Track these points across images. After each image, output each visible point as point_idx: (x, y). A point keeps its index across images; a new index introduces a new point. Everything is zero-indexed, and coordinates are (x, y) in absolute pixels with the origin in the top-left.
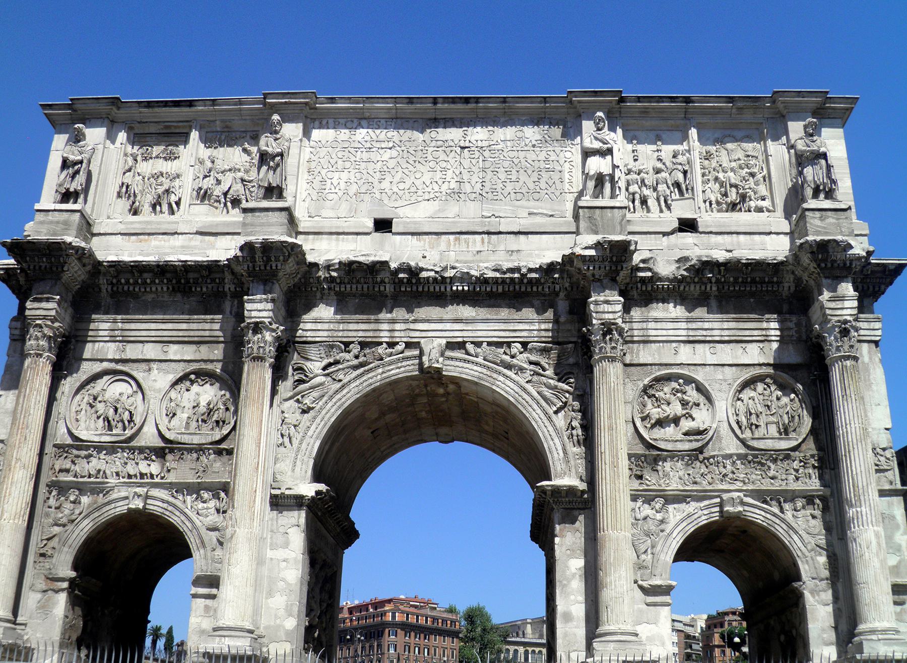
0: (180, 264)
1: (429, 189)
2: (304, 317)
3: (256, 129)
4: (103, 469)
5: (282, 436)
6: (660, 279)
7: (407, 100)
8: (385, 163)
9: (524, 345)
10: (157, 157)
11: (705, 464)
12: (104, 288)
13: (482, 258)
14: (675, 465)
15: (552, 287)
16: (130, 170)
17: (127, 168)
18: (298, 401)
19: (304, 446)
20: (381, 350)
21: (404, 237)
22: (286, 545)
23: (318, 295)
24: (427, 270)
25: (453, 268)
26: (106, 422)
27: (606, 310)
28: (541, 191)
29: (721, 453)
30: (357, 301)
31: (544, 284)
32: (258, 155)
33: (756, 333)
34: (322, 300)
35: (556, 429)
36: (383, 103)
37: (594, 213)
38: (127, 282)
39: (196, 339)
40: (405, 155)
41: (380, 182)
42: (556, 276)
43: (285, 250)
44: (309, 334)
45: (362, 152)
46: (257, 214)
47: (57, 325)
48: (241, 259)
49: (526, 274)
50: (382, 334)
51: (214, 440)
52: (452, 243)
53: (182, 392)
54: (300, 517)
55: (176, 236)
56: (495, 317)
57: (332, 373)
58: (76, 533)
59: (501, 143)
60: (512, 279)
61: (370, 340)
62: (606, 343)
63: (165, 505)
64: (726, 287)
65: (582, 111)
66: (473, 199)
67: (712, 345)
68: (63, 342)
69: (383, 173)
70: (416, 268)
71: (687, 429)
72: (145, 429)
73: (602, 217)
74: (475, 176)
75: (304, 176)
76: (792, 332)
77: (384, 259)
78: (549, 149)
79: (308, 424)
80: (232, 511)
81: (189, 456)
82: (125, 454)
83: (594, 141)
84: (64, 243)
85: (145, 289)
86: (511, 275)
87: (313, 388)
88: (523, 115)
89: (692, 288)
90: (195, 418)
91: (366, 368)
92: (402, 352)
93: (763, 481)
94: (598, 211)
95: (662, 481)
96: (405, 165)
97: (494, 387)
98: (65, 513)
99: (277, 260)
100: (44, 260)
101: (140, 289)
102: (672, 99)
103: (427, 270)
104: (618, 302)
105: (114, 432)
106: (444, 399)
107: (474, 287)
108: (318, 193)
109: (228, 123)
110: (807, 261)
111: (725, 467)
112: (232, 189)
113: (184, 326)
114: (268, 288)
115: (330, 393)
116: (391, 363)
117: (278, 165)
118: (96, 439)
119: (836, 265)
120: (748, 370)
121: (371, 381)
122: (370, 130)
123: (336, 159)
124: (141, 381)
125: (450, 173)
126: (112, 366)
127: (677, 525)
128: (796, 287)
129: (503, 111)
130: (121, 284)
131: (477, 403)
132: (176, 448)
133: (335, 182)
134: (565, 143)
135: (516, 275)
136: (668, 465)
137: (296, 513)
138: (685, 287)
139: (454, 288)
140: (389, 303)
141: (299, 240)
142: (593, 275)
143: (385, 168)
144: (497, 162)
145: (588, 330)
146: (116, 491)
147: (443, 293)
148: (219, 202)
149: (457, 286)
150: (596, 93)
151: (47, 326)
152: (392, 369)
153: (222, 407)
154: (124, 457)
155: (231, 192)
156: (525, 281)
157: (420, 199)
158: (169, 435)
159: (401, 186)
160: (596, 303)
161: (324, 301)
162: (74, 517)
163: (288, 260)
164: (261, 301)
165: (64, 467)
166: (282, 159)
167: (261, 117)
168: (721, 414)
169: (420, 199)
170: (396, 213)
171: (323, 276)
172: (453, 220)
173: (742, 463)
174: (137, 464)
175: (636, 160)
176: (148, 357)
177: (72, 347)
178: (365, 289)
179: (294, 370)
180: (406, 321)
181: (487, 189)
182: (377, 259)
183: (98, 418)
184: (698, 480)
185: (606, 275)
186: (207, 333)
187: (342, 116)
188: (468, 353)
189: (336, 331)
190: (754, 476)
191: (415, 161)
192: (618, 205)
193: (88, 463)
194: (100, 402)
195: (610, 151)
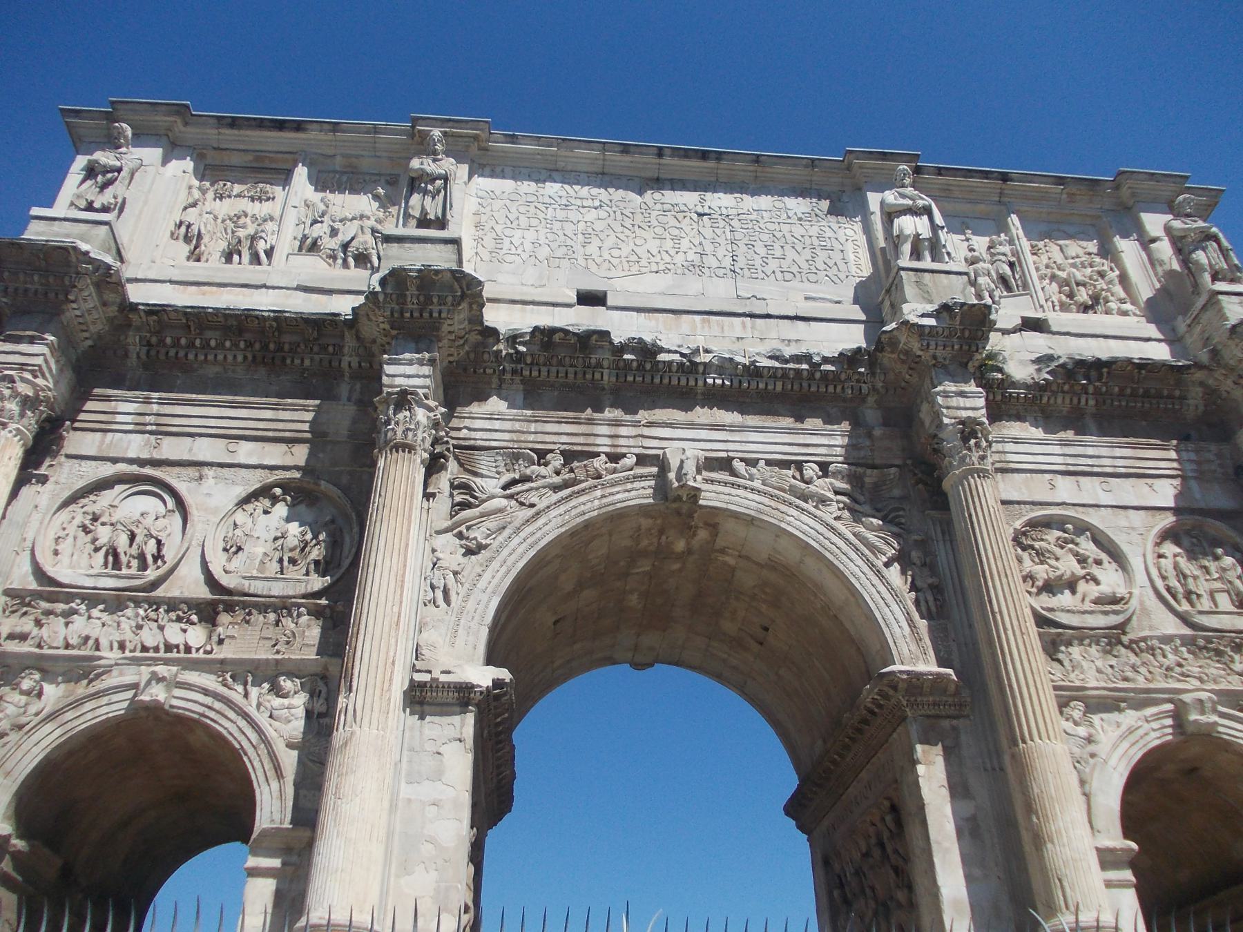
0: (272, 314)
1: (658, 259)
4: (94, 635)
5: (433, 587)
6: (1014, 384)
7: (621, 148)
8: (589, 224)
10: (238, 196)
11: (1133, 651)
14: (1086, 651)
16: (194, 205)
17: (191, 200)
18: (460, 536)
19: (471, 605)
20: (599, 463)
22: (437, 775)
24: (669, 352)
25: (707, 351)
26: (111, 559)
29: (1157, 633)
35: (891, 589)
39: (287, 434)
40: (619, 217)
41: (584, 246)
42: (863, 370)
44: (479, 435)
47: (40, 381)
48: (381, 298)
49: (820, 365)
50: (599, 441)
51: (309, 590)
52: (699, 325)
53: (256, 514)
54: (466, 724)
55: (264, 290)
57: (518, 494)
58: (25, 747)
60: (798, 371)
61: (579, 448)
62: (969, 449)
63: (208, 700)
64: (1109, 401)
65: (865, 179)
66: (722, 275)
67: (1102, 479)
68: (48, 419)
71: (1097, 595)
72: (182, 570)
74: (722, 248)
79: (479, 570)
80: (347, 698)
81: (261, 618)
82: (141, 612)
84: (75, 249)
85: (206, 356)
86: (797, 366)
89: (1059, 400)
90: (277, 555)
91: (576, 488)
92: (631, 470)
93: (1230, 678)
95: (1072, 676)
97: (783, 525)
98: (8, 712)
99: (442, 301)
100: (36, 278)
101: (196, 355)
102: (986, 175)
103: (669, 352)
105: (124, 571)
106: (676, 566)
107: (740, 381)
108: (491, 252)
109: (354, 160)
111: (1164, 656)
113: (268, 414)
115: (517, 523)
116: (615, 484)
117: (439, 192)
118: (89, 582)
120: (1162, 516)
121: (582, 508)
122: (566, 186)
123: (516, 214)
125: (685, 244)
126: (134, 469)
127: (1115, 746)
128: (1206, 406)
129: (755, 174)
130: (165, 345)
131: (733, 570)
132: (238, 603)
133: (516, 242)
135: (805, 366)
136: (1075, 651)
137: (456, 719)
138: (1049, 399)
143: (590, 231)
146: (115, 672)
149: (714, 379)
151: (23, 380)
152: (618, 493)
154: (137, 615)
155: (353, 244)
156: (818, 375)
157: (644, 270)
158: (225, 581)
159: (616, 253)
160: (946, 395)
162: (23, 720)
163: (459, 304)
164: (410, 363)
165: (18, 630)
168: (1140, 577)
169: (644, 270)
171: (504, 353)
173: (1189, 652)
174: (161, 628)
176: (201, 458)
178: (571, 376)
179: (453, 487)
183: (97, 550)
184: (1129, 674)
188: (734, 473)
189: (523, 433)
190: (1214, 671)
191: (633, 225)
193: (67, 624)
194: (103, 524)
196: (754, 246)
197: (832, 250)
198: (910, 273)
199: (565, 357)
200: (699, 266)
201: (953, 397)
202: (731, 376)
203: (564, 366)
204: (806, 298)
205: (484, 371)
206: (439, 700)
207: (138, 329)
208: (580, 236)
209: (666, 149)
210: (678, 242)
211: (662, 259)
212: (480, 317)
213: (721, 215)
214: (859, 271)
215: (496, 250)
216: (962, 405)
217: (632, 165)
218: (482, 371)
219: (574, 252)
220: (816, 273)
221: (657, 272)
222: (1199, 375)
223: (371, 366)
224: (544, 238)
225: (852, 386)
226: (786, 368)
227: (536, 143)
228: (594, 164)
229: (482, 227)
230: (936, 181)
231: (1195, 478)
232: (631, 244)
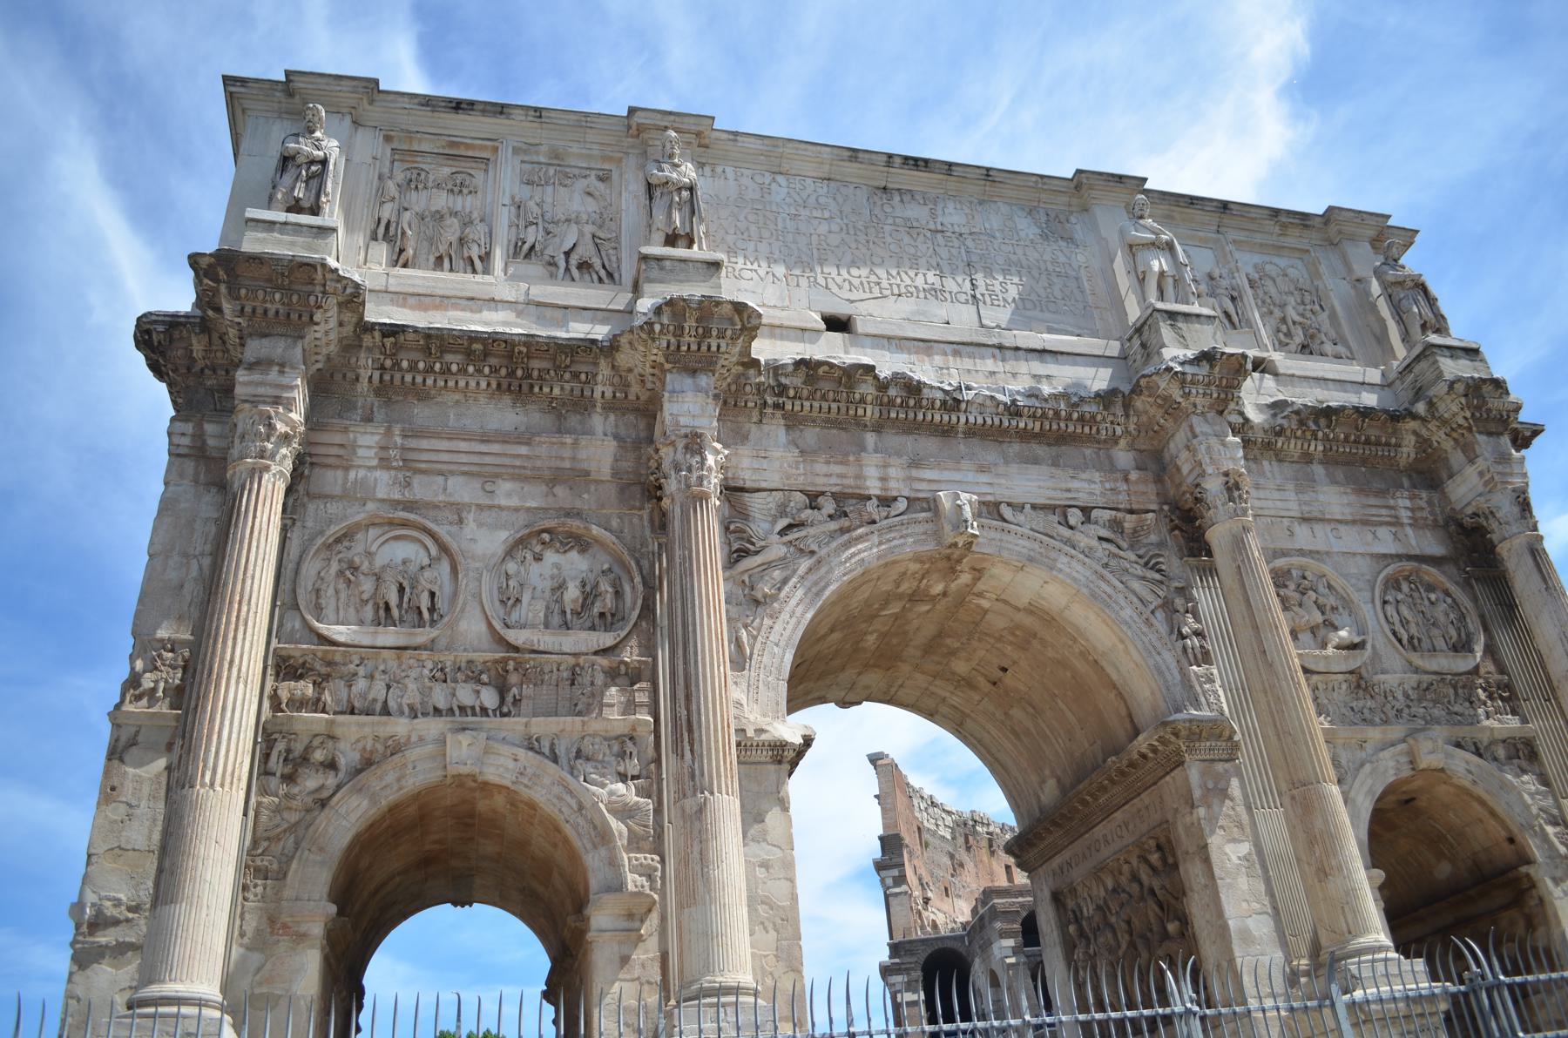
3: (607, 167)
9: (1086, 511)
10: (438, 186)
12: (364, 374)
20: (871, 506)
25: (968, 388)
26: (382, 613)
33: (1384, 512)
38: (413, 367)
60: (1057, 413)
64: (1335, 448)
76: (1425, 514)
84: (324, 265)
87: (768, 565)
89: (1293, 442)
96: (854, 245)
99: (721, 335)
100: (277, 296)
101: (435, 381)
110: (1455, 408)
112: (579, 250)
116: (890, 528)
119: (1492, 415)
124: (447, 539)
130: (401, 369)
131: (986, 612)
148: (552, 264)
152: (894, 538)
153: (610, 590)
156: (1075, 416)
169: (886, 292)
177: (306, 472)
185: (1211, 407)
186: (567, 464)
195: (1170, 247)
206: (758, 759)
207: (369, 349)
222: (1413, 424)
223: (626, 396)
231: (1410, 525)
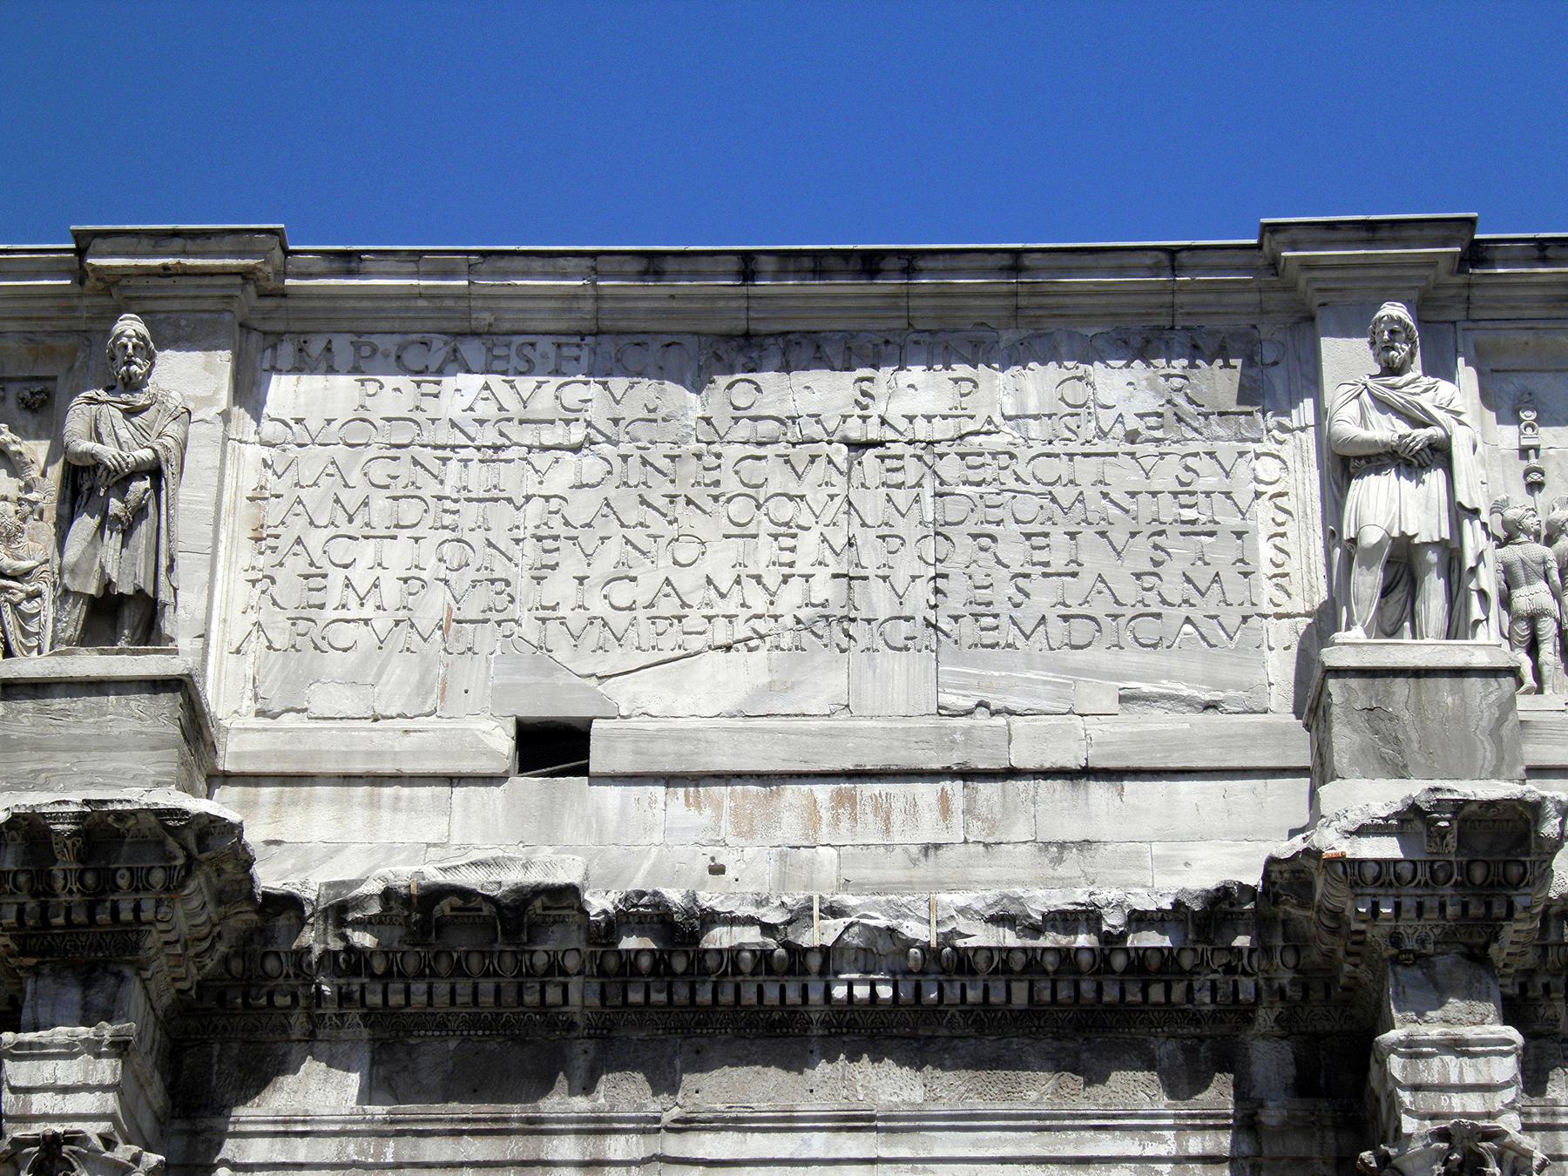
1: (731, 606)
2: (241, 1112)
7: (639, 265)
8: (554, 504)
13: (945, 874)
15: (1225, 988)
21: (636, 791)
23: (298, 1023)
24: (733, 921)
25: (834, 911)
27: (1454, 1079)
28: (1164, 610)
30: (452, 1045)
31: (1191, 973)
32: (55, 472)
34: (311, 1042)
36: (545, 275)
37: (1389, 693)
40: (635, 473)
42: (1242, 941)
43: (172, 844)
45: (466, 462)
46: (59, 703)
49: (1123, 936)
52: (826, 816)
56: (1002, 1107)
59: (1006, 427)
60: (1067, 956)
65: (1318, 299)
66: (900, 643)
69: (549, 544)
70: (688, 912)
73: (1419, 709)
74: (909, 552)
75: (237, 556)
77: (560, 878)
78: (1193, 447)
83: (1374, 415)
86: (1063, 941)
88: (1087, 317)
94: (1401, 686)
96: (633, 514)
99: (140, 883)
103: (733, 921)
104: (1493, 1048)
107: (918, 988)
108: (294, 621)
114: (99, 999)
117: (140, 512)
122: (495, 380)
125: (808, 544)
129: (1010, 302)
134: (1252, 425)
135: (1083, 940)
139: (839, 992)
140: (581, 1053)
141: (222, 805)
142: (1395, 939)
143: (556, 522)
144: (990, 501)
145: (1385, 1160)
147: (793, 1011)
149: (850, 984)
150: (1371, 231)
156: (1119, 961)
157: (695, 643)
159: (622, 593)
160: (1413, 1050)
161: (321, 1047)
163: (182, 885)
164: (69, 1052)
166: (157, 488)
167: (63, 325)
169: (695, 643)
170: (604, 700)
171: (317, 949)
172: (827, 723)
175: (1534, 487)
178: (487, 999)
180: (649, 1126)
181: (954, 604)
182: (534, 877)
185: (1447, 939)
187: (383, 325)
191: (672, 498)
192: (1481, 659)
195: (1439, 454)
196: (993, 539)
197: (1211, 534)
198: (1354, 683)
199: (468, 953)
200: (840, 620)
201: (1432, 1055)
202: (893, 973)
203: (468, 977)
204: (1123, 699)
205: (270, 996)
208: (530, 545)
209: (763, 258)
210: (789, 542)
211: (743, 605)
212: (245, 886)
213: (910, 443)
214: (1280, 597)
215: (306, 613)
216: (1454, 1079)
217: (674, 304)
218: (263, 1001)
219: (512, 601)
220: (1158, 616)
221: (728, 648)
224: (434, 560)
225: (1213, 982)
226: (1034, 949)
227: (411, 267)
228: (570, 310)
229: (271, 542)
230: (1534, 279)
232: (665, 562)
